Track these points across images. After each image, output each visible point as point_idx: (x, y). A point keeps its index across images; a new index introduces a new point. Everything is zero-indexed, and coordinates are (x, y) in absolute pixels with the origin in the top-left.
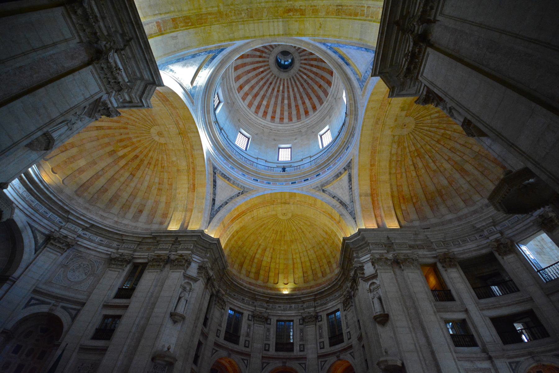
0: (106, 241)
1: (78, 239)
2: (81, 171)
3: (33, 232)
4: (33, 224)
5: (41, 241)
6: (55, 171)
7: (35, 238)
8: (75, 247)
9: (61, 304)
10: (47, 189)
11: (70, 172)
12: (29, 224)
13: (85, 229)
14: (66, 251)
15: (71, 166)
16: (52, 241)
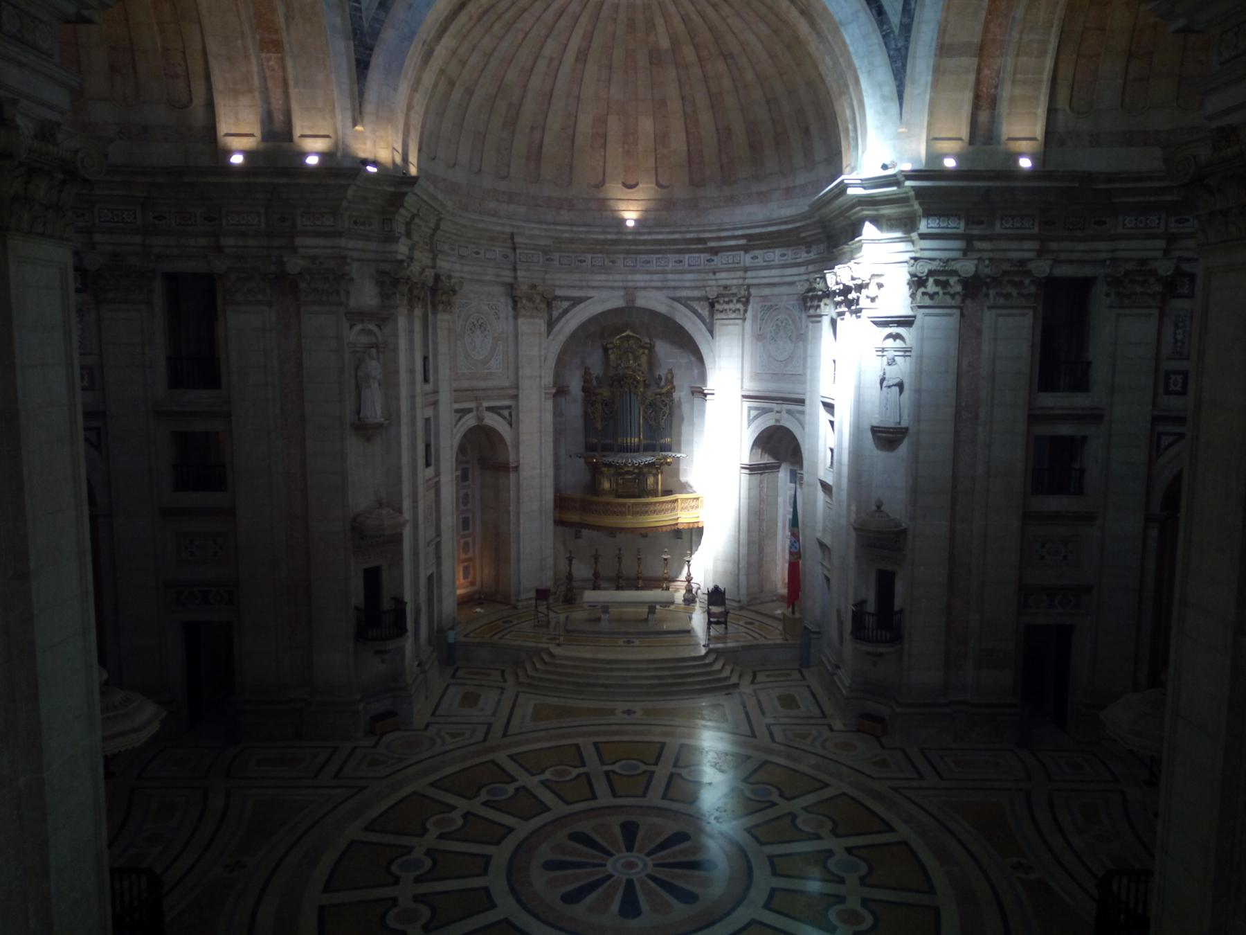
0: (789, 252)
1: (749, 274)
2: (661, 138)
3: (686, 306)
4: (679, 294)
5: (705, 313)
6: (633, 183)
7: (695, 312)
8: (753, 291)
9: (786, 407)
10: (640, 234)
11: (651, 161)
12: (673, 299)
13: (746, 249)
14: (745, 311)
16: (717, 306)
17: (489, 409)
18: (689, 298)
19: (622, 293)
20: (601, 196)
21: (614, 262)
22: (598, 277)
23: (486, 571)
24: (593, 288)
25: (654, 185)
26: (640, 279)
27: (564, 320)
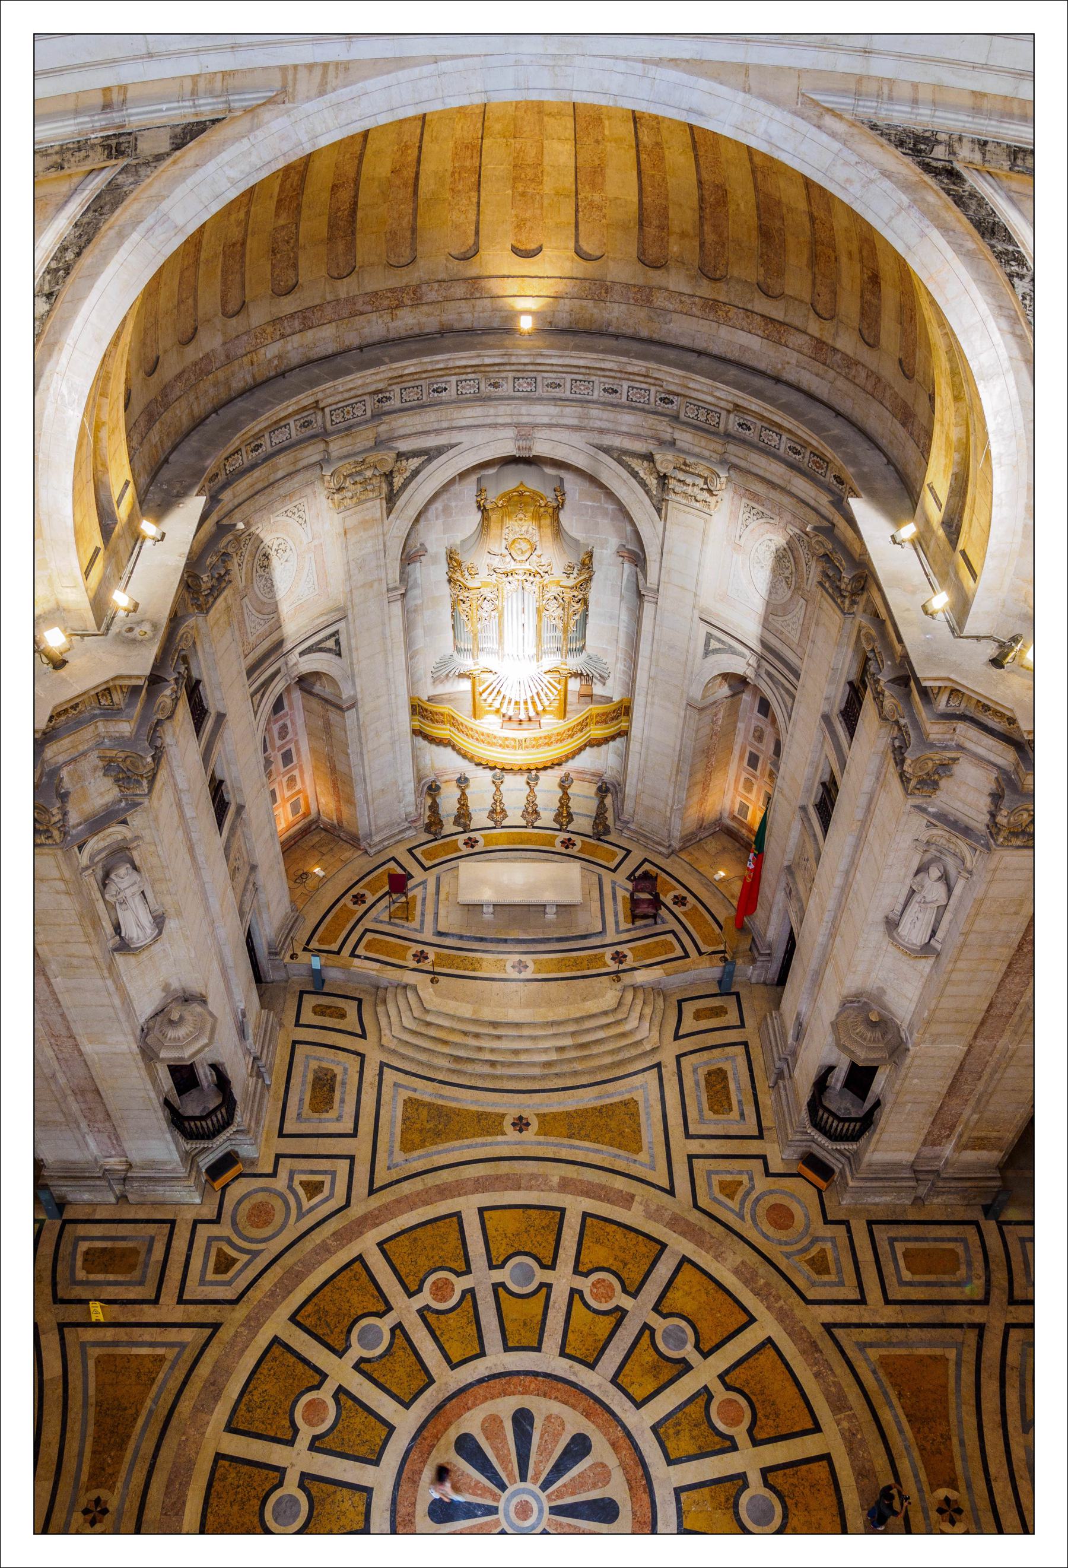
3: (620, 462)
4: (608, 440)
6: (533, 246)
7: (635, 474)
12: (600, 448)
15: (548, 187)
17: (302, 654)
18: (626, 452)
19: (510, 433)
20: (473, 271)
21: (496, 385)
22: (469, 412)
23: (322, 800)
24: (461, 428)
25: (572, 253)
26: (542, 412)
27: (413, 485)
